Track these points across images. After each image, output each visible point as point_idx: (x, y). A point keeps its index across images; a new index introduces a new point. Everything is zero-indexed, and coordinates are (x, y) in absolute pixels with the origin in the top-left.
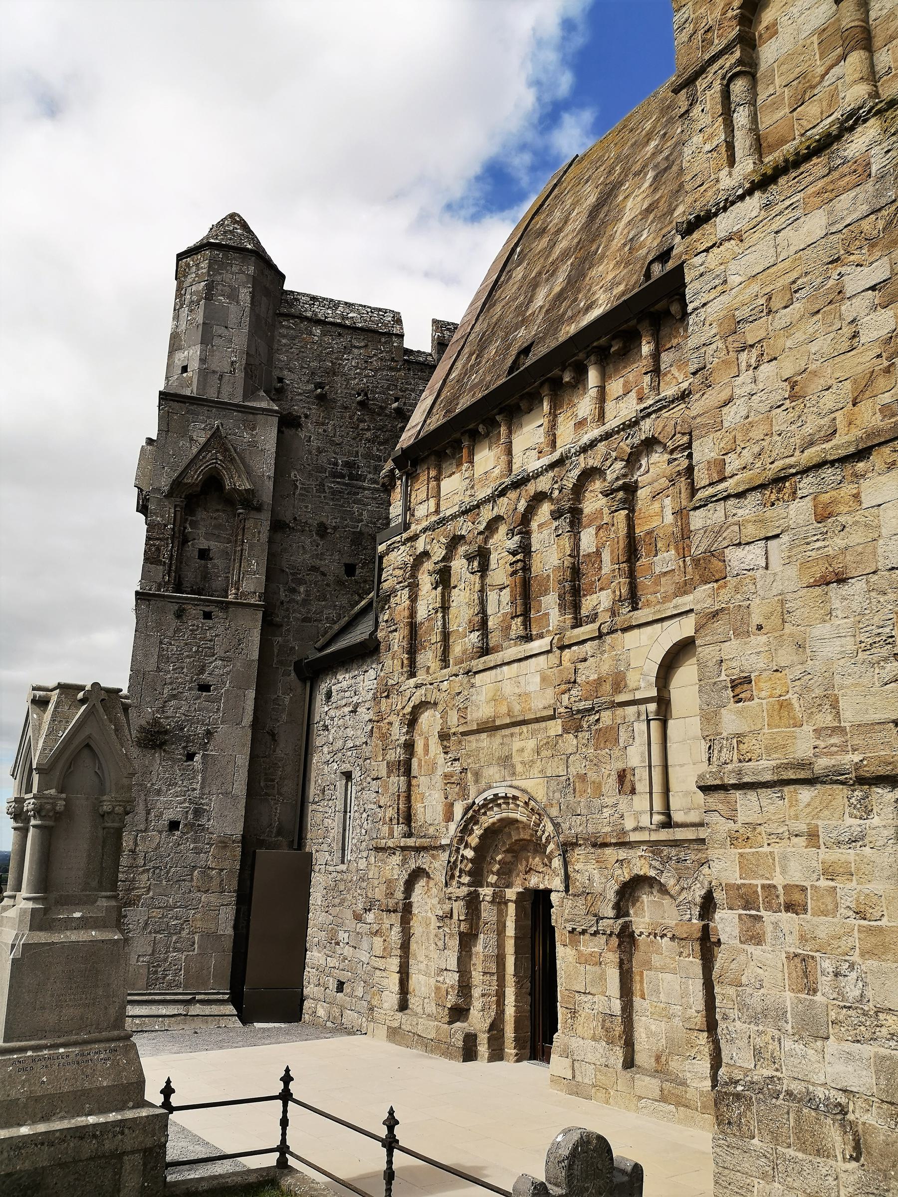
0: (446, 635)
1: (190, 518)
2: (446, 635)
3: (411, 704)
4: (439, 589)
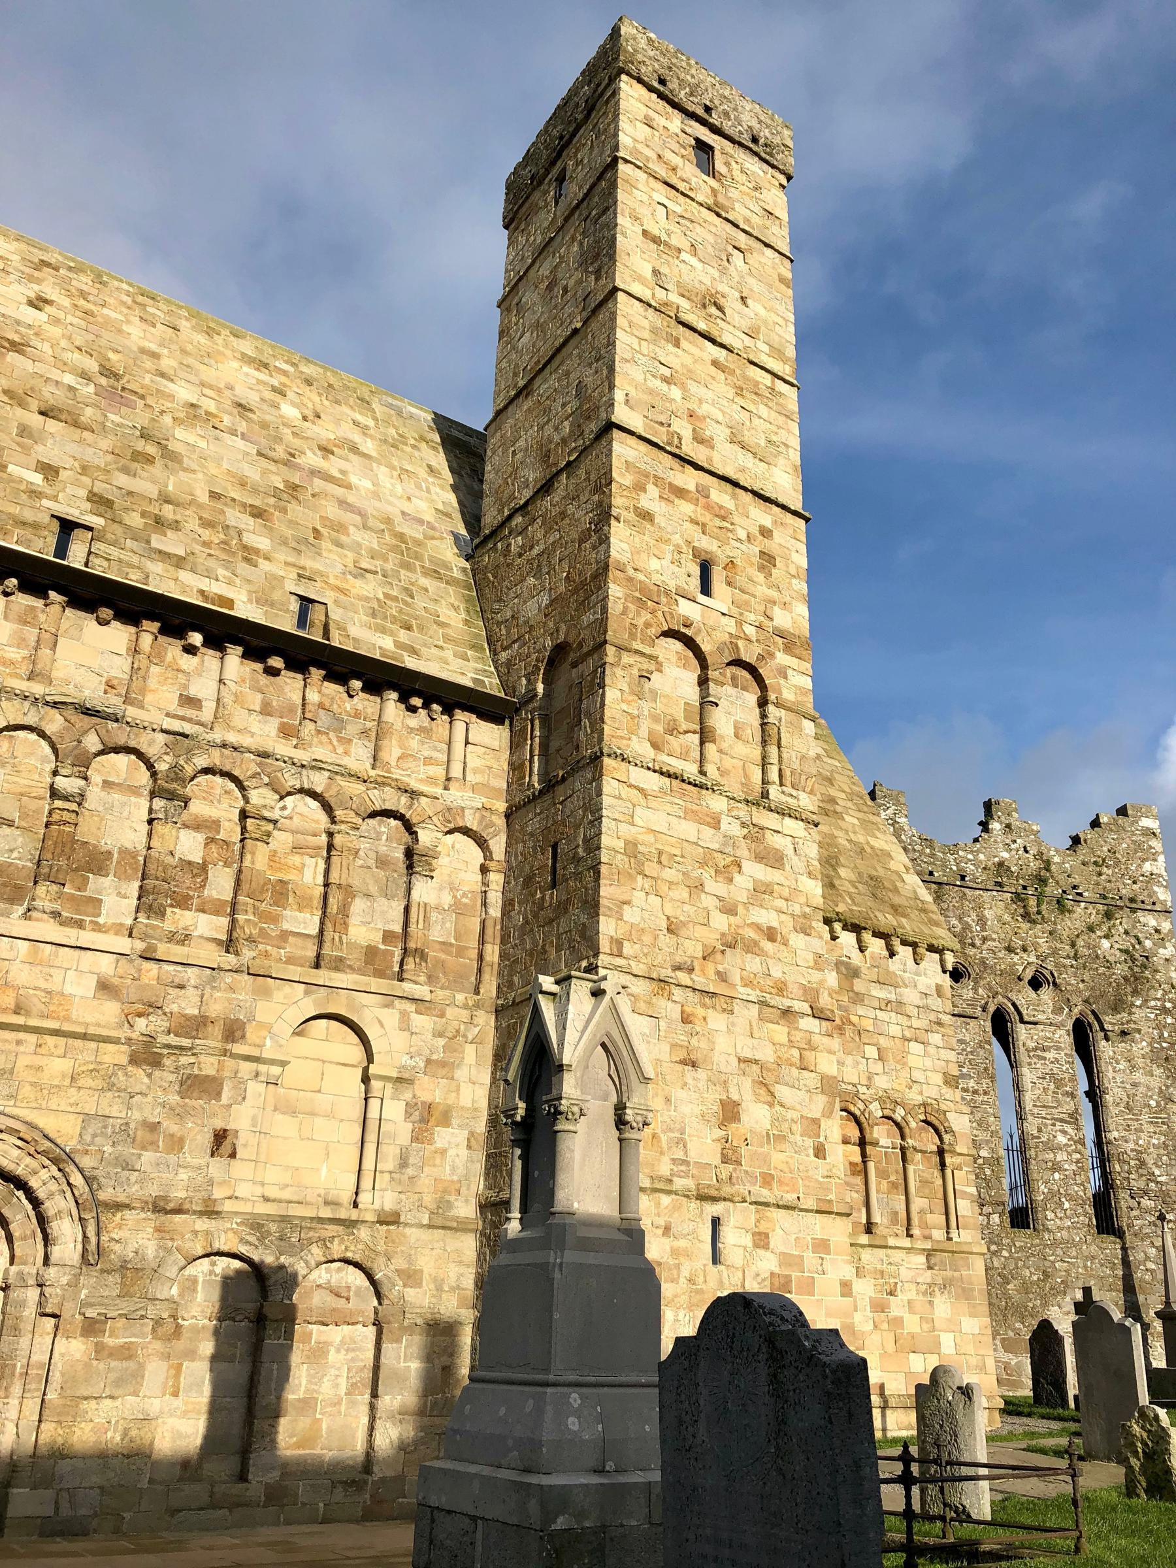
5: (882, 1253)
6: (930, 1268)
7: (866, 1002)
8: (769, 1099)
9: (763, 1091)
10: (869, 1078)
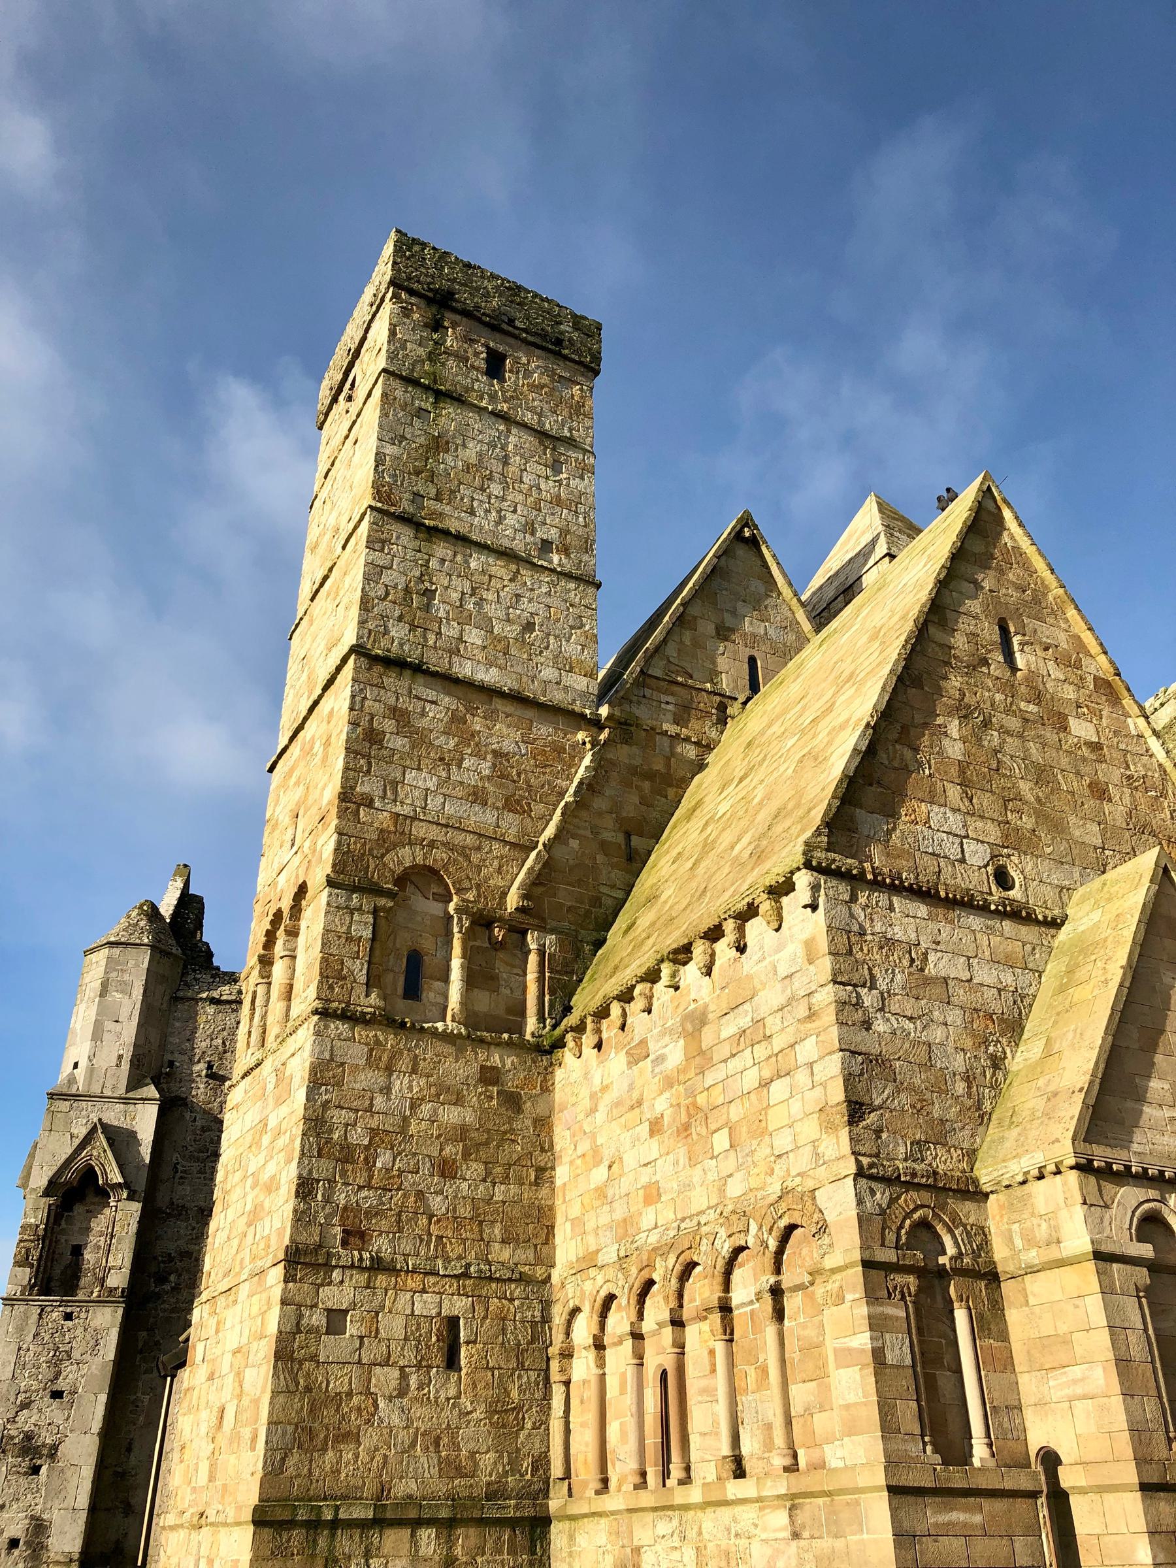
1: (66, 1214)
5: (725, 1513)
6: (796, 1535)
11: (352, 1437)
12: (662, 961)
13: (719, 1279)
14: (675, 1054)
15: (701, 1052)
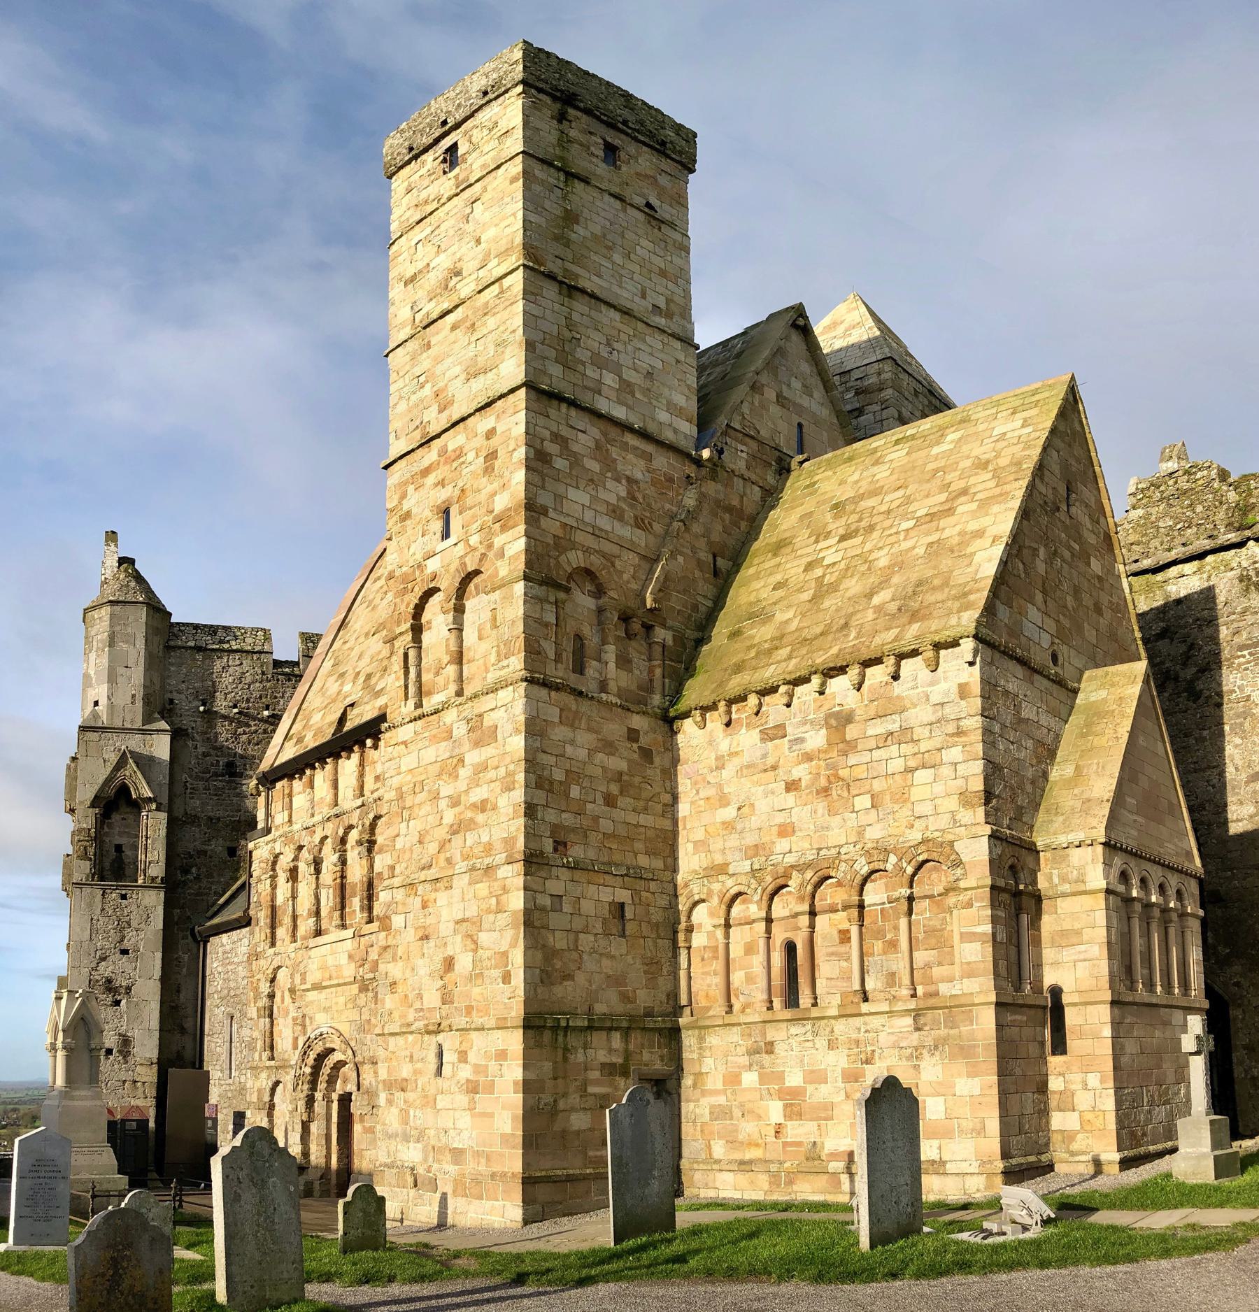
0: (295, 918)
2: (295, 918)
3: (272, 967)
4: (290, 883)
7: (859, 748)
8: (473, 946)
9: (469, 942)
10: (859, 833)
11: (569, 977)
12: (815, 673)
13: (857, 888)
14: (816, 739)
15: (844, 741)
